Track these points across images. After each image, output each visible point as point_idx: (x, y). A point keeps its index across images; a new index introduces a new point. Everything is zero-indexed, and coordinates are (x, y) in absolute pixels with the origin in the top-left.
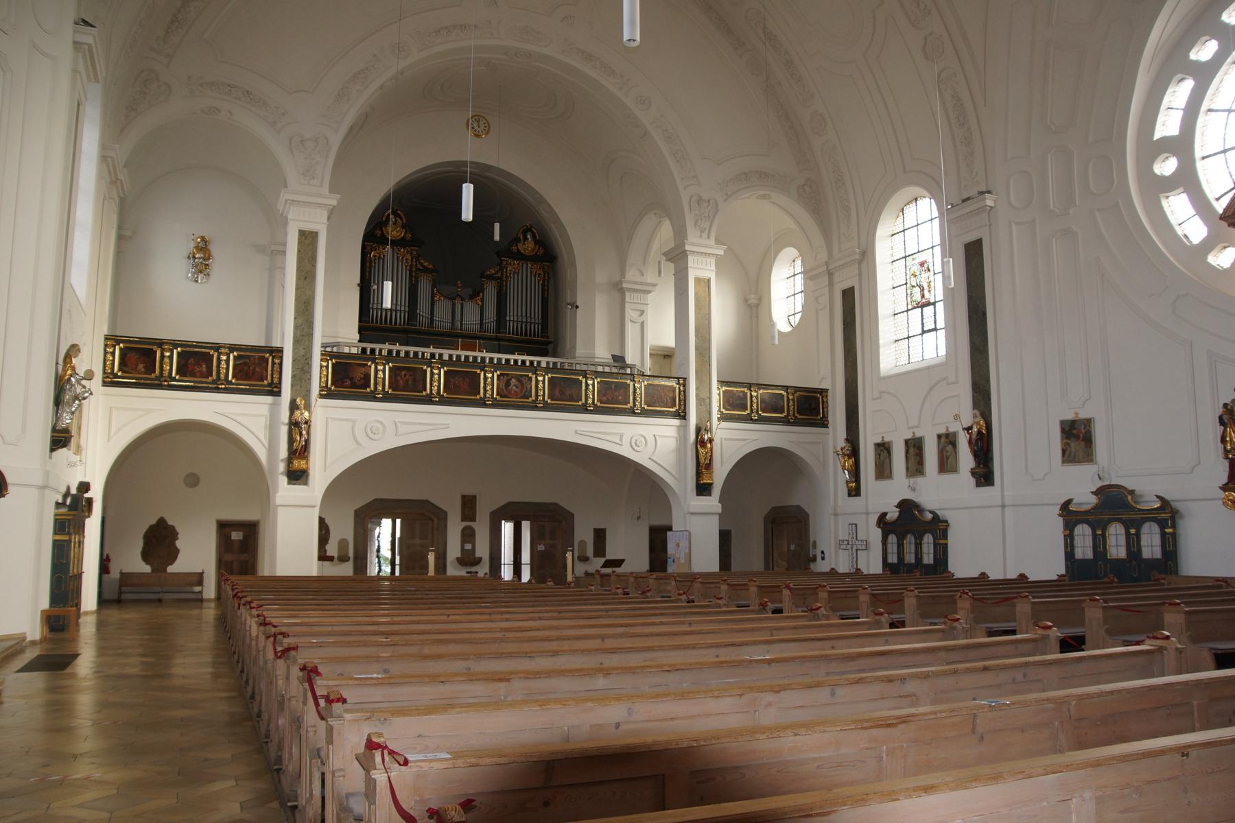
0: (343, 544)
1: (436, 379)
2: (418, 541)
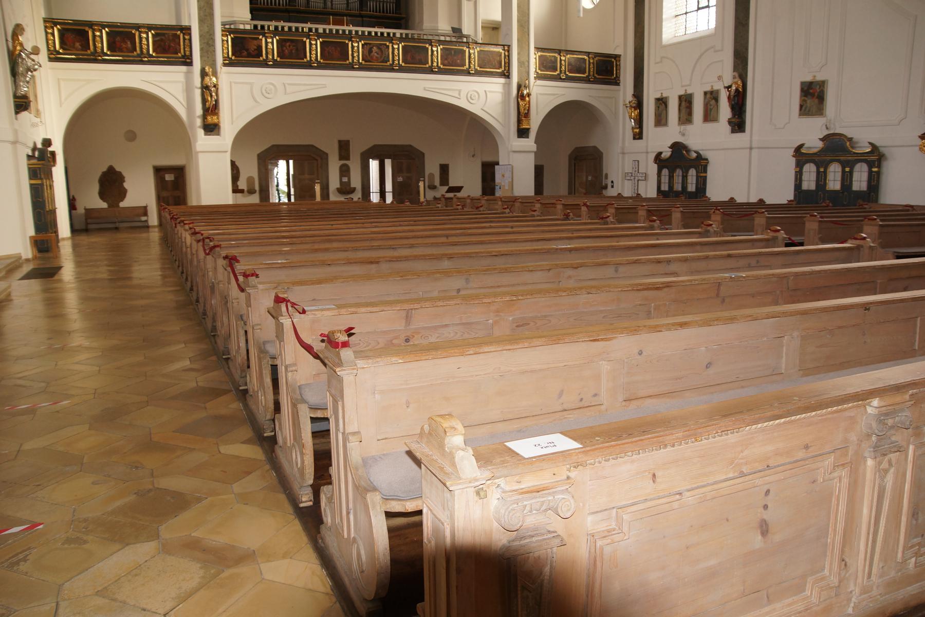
0: (250, 180)
1: (314, 49)
2: (307, 176)
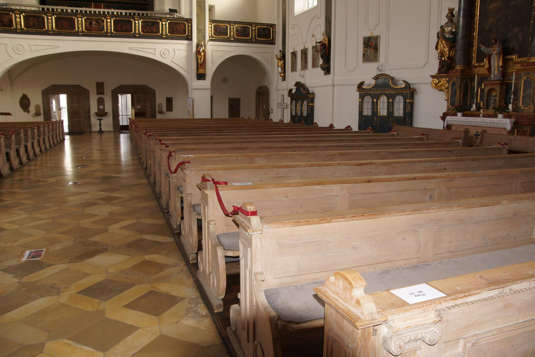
0: (37, 107)
1: (81, 23)
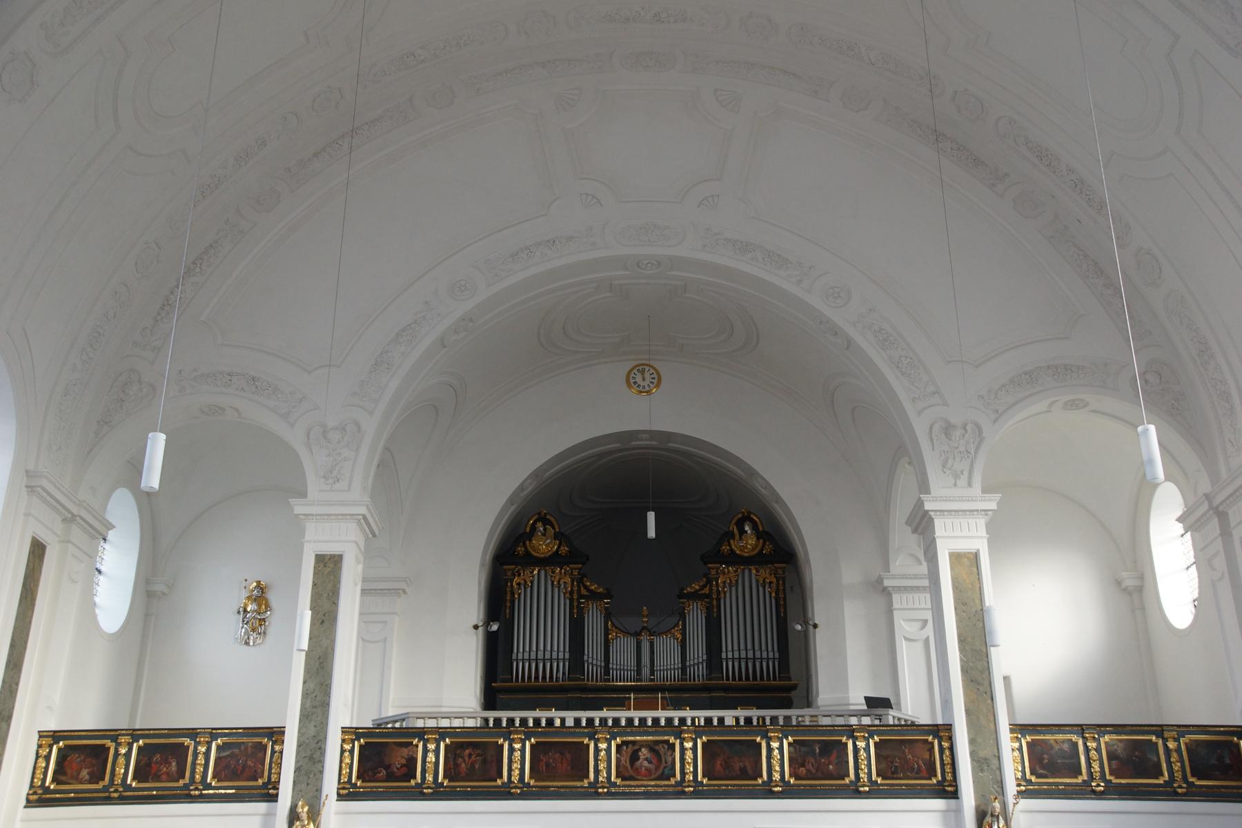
1: (603, 756)
